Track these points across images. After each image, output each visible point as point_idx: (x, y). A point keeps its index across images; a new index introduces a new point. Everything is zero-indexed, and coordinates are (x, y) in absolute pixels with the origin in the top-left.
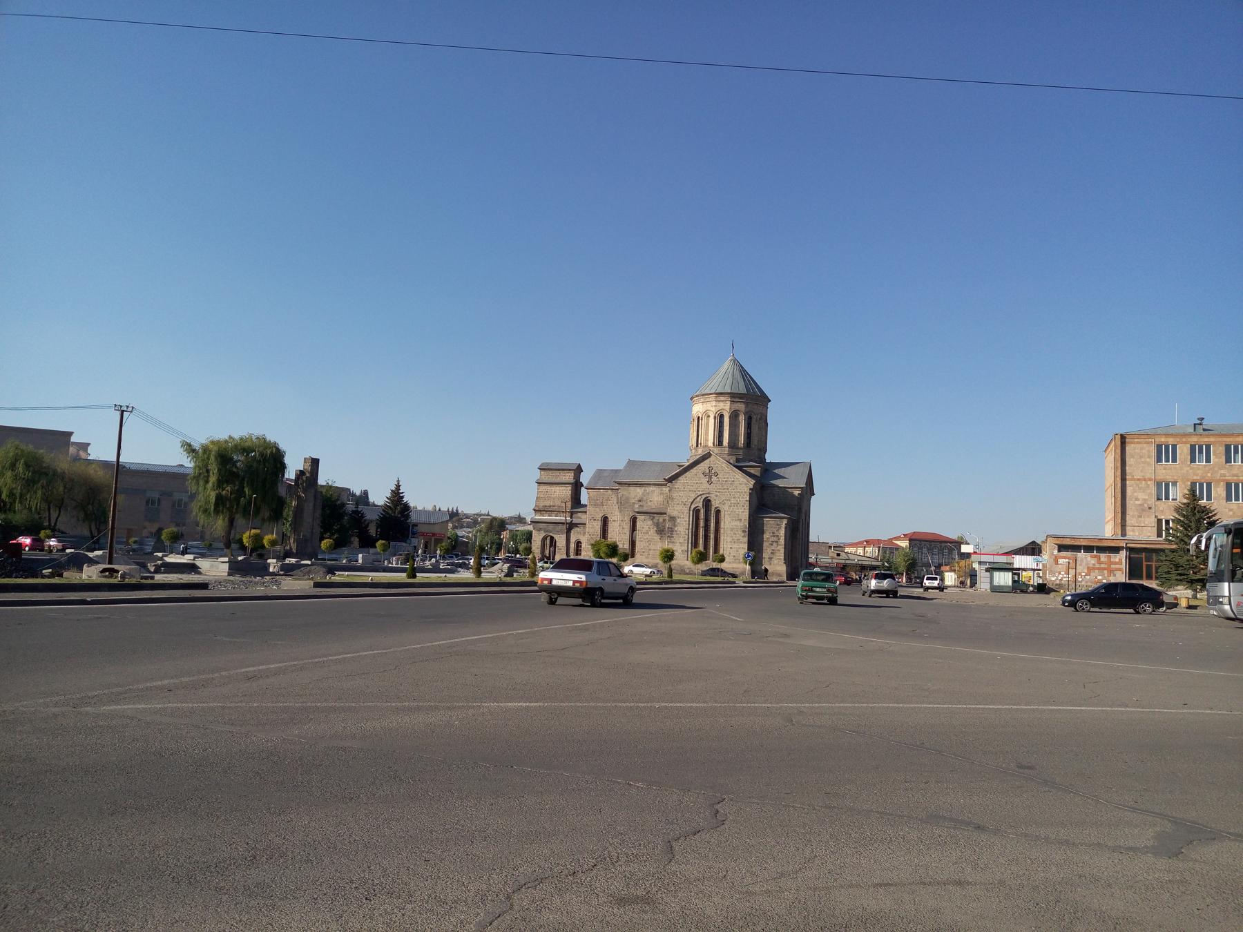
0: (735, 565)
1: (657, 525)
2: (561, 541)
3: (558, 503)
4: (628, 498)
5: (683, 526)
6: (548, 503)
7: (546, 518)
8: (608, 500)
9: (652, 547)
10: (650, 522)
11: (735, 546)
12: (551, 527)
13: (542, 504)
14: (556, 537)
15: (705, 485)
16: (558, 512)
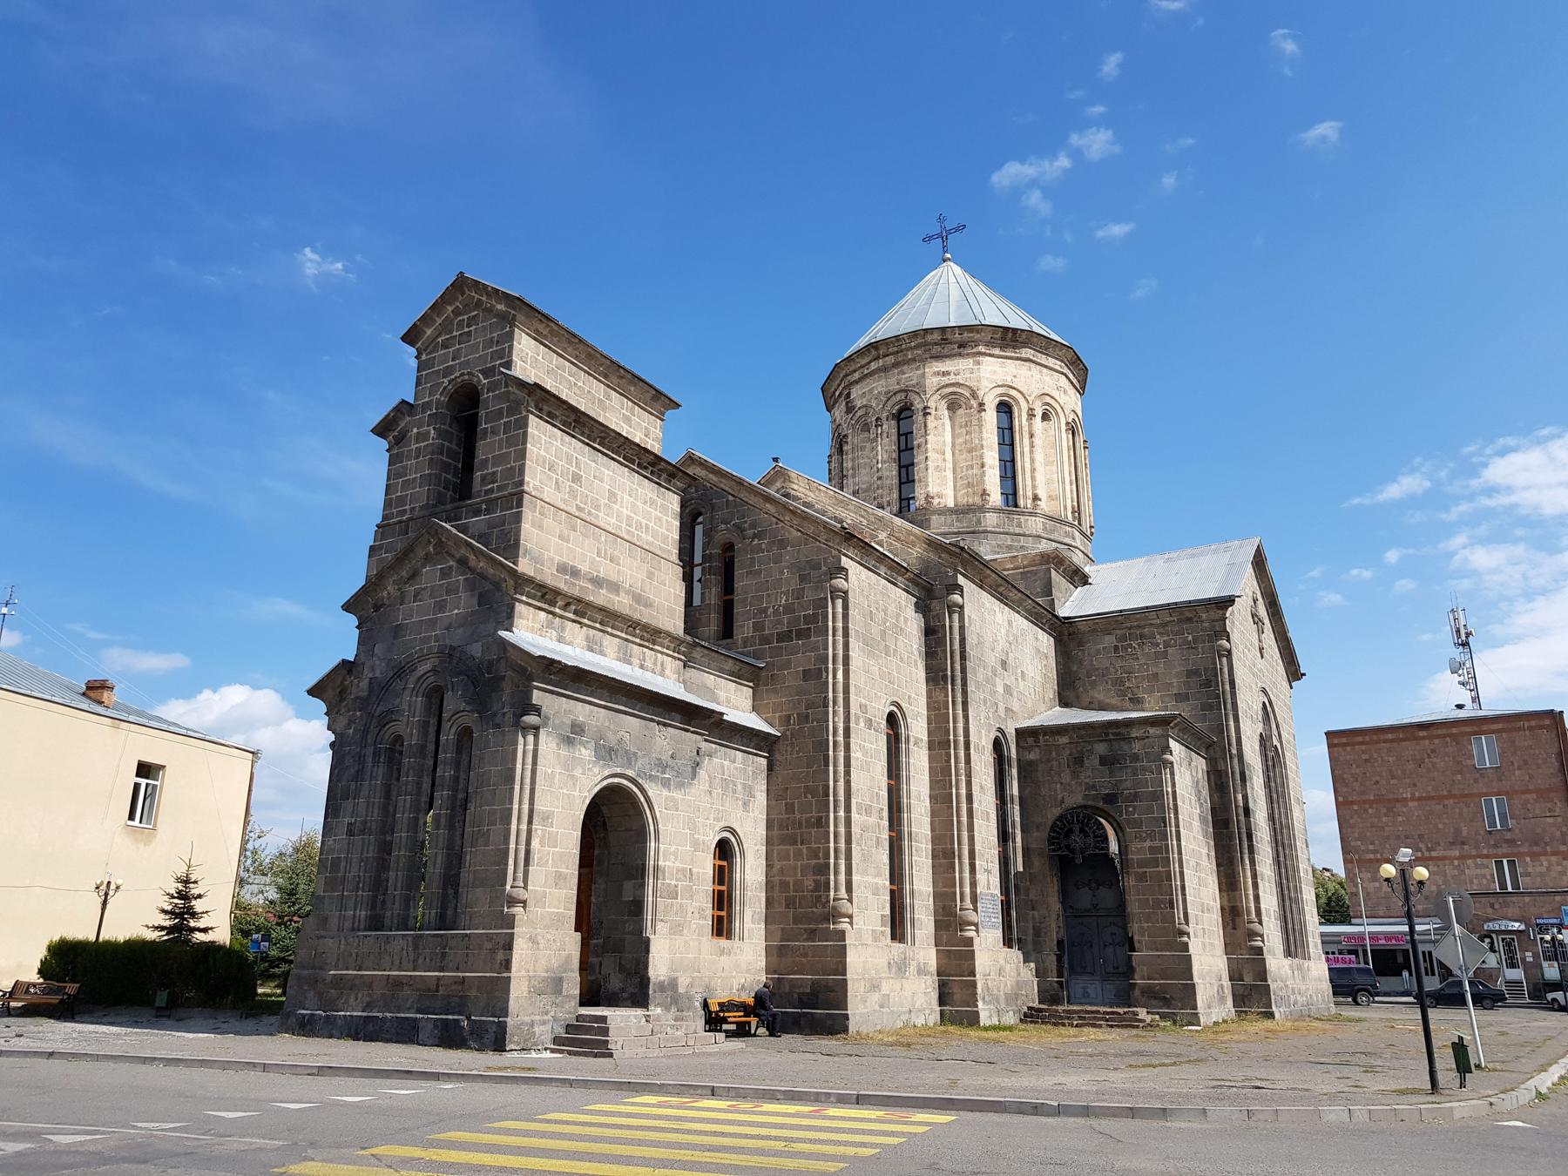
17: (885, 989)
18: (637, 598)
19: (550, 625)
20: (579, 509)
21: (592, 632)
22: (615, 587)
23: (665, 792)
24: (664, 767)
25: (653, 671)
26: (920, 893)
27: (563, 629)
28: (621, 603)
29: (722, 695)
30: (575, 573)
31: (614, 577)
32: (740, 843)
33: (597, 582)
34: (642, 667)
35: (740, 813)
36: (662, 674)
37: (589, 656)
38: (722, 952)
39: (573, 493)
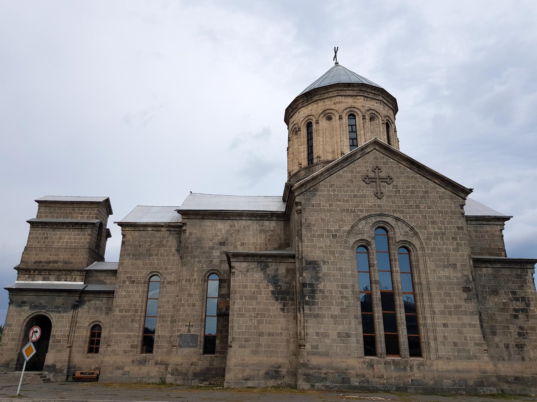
0: (462, 365)
1: (274, 280)
2: (60, 323)
3: (63, 256)
4: (199, 240)
5: (341, 279)
6: (44, 257)
7: (39, 283)
8: (161, 245)
9: (266, 328)
10: (258, 275)
11: (453, 320)
12: (43, 300)
13: (33, 258)
14: (54, 317)
15: (371, 201)
16: (66, 272)
17: (126, 369)
18: (65, 263)
19: (29, 277)
20: (46, 245)
21: (45, 276)
22: (56, 262)
23: (58, 314)
24: (58, 307)
25: (70, 281)
26: (163, 336)
27: (34, 277)
28: (60, 265)
29: (108, 281)
30: (40, 262)
31: (57, 259)
32: (104, 325)
33: (49, 262)
34: (65, 281)
35: (104, 316)
36: (75, 281)
37: (45, 282)
38: (89, 358)
39: (44, 242)
